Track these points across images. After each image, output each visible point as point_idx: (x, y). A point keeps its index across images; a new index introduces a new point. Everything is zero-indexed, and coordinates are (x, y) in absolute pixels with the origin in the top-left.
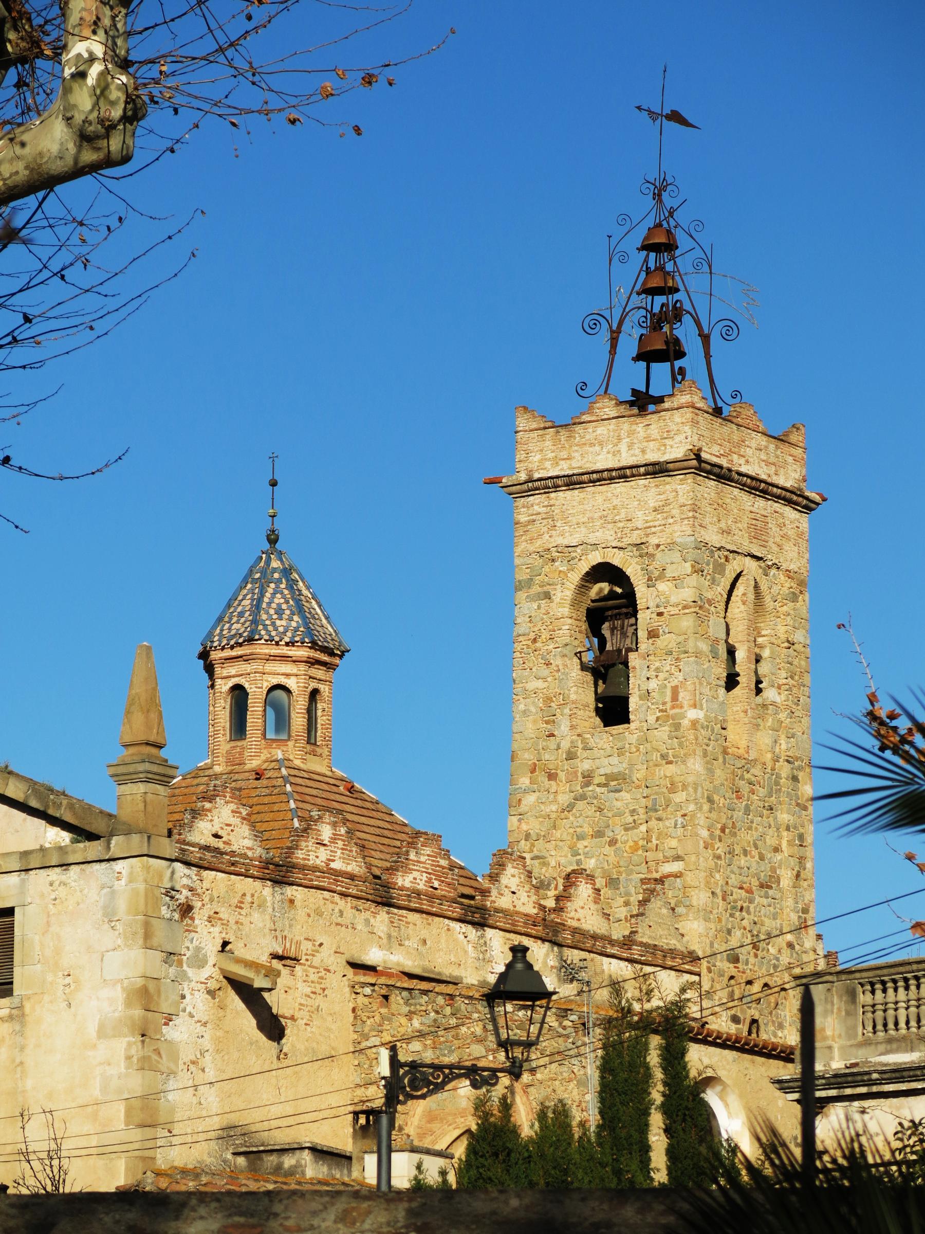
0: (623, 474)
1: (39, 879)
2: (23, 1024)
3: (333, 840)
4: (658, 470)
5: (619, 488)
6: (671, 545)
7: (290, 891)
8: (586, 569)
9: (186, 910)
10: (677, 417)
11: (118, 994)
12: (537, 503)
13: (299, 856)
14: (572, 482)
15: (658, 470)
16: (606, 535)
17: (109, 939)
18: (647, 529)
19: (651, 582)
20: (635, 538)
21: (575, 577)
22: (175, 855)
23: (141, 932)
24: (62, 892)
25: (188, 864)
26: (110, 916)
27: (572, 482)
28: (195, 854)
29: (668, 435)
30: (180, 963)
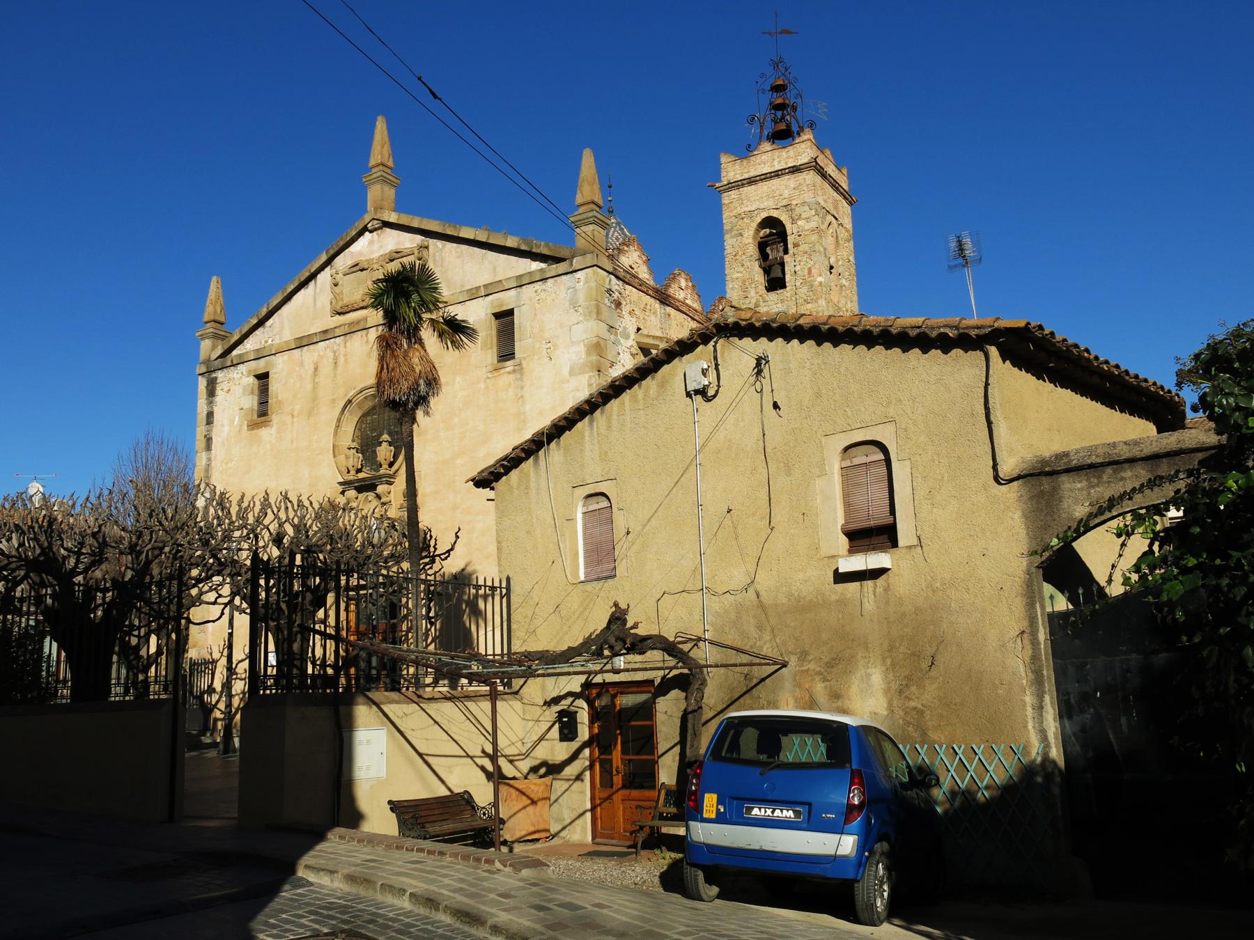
0: (777, 174)
1: (528, 290)
2: (522, 374)
3: (687, 287)
4: (795, 170)
5: (775, 182)
6: (804, 203)
7: (669, 309)
8: (759, 220)
9: (618, 304)
10: (803, 146)
11: (582, 349)
12: (733, 194)
13: (671, 291)
14: (751, 181)
15: (795, 170)
16: (771, 204)
17: (575, 317)
18: (791, 198)
19: (793, 222)
20: (785, 202)
21: (755, 225)
22: (611, 270)
23: (595, 311)
24: (543, 295)
25: (618, 277)
26: (574, 305)
27: (751, 181)
28: (621, 274)
29: (799, 154)
30: (616, 334)
